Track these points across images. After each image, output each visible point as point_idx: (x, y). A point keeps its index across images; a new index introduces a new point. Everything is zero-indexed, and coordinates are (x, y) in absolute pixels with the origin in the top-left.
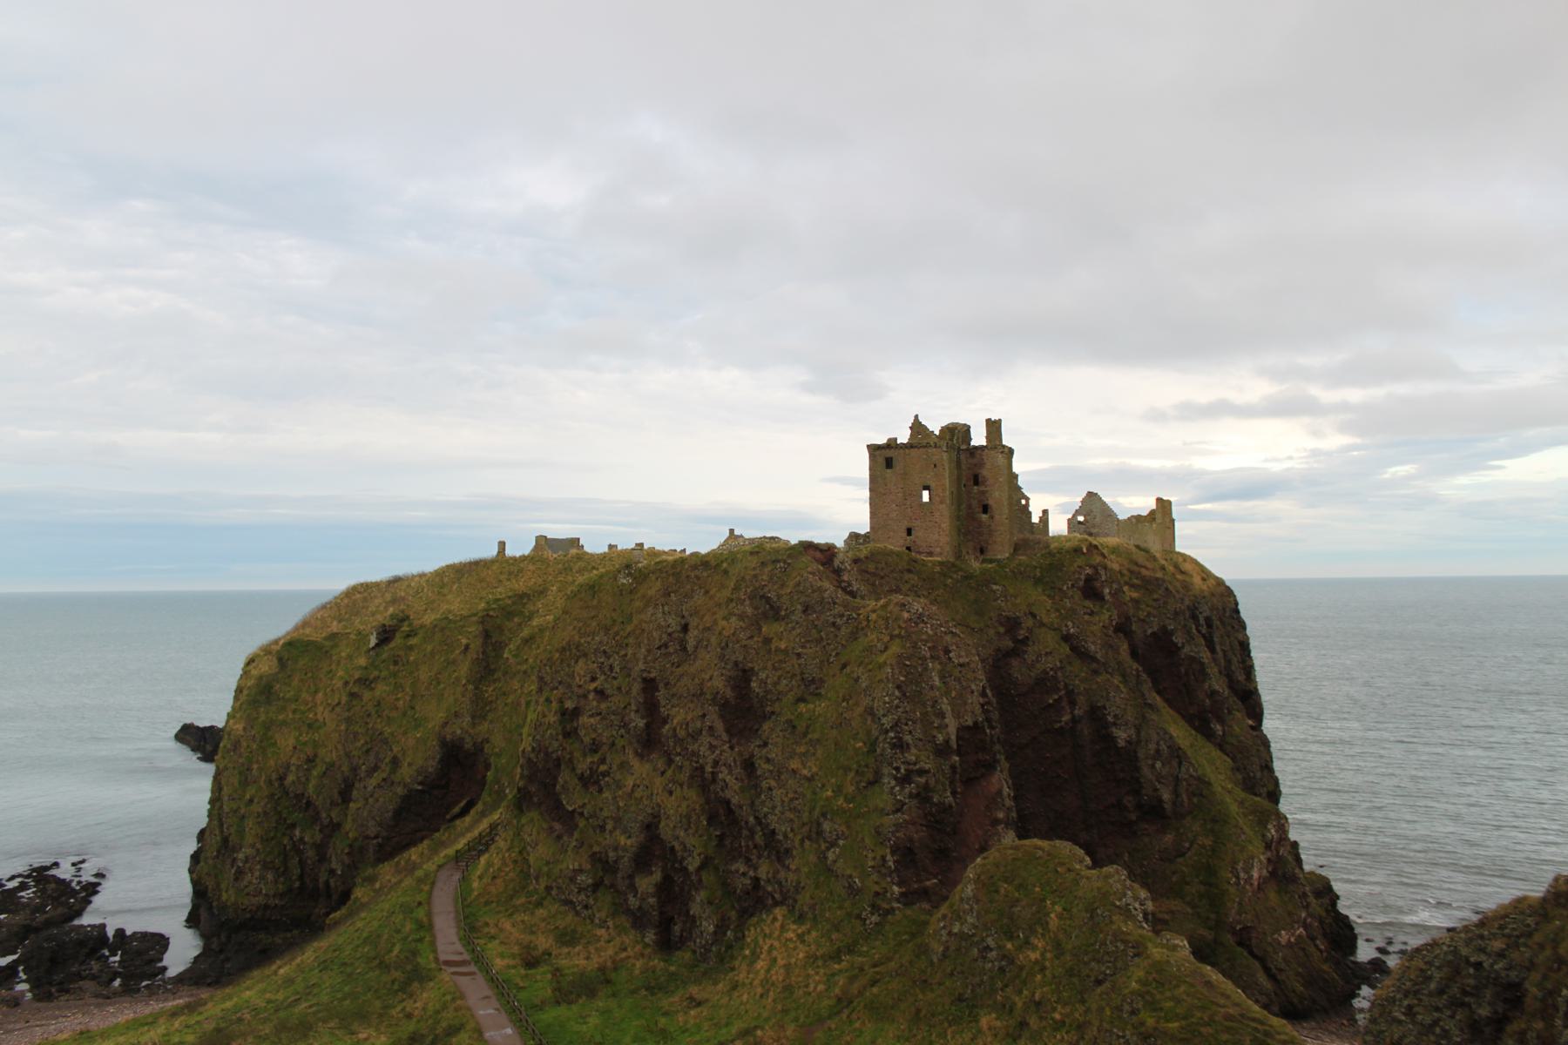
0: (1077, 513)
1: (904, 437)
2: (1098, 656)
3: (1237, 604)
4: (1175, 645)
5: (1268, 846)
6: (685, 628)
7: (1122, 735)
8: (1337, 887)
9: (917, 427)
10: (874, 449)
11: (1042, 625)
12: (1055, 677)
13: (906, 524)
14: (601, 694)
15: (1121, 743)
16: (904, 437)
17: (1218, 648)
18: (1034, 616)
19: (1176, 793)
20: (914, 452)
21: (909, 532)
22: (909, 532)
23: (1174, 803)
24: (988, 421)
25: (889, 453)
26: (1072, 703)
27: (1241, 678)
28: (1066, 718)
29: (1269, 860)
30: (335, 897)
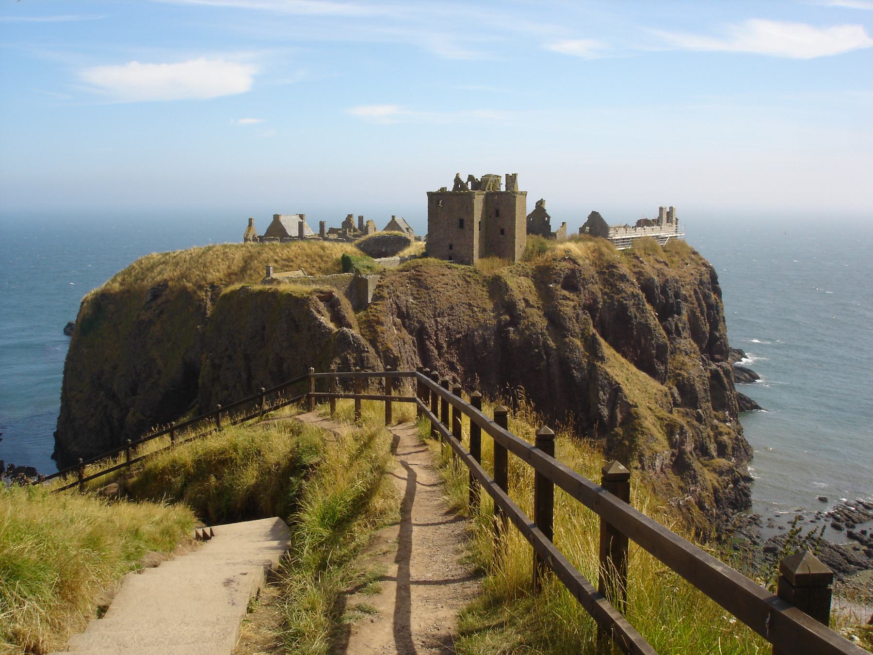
0: (585, 225)
1: (450, 188)
3: (714, 278)
4: (630, 318)
5: (672, 445)
6: (264, 328)
9: (457, 180)
10: (430, 195)
11: (532, 307)
12: (538, 338)
14: (230, 357)
16: (450, 188)
17: (684, 312)
18: (526, 301)
21: (451, 247)
22: (451, 247)
24: (507, 175)
26: (548, 354)
27: (707, 328)
28: (543, 363)
29: (673, 455)
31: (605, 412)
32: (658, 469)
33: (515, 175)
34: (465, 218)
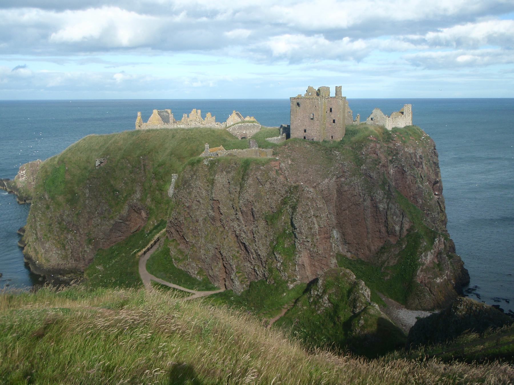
2: (374, 177)
7: (381, 206)
8: (463, 259)
13: (304, 128)
15: (381, 209)
19: (401, 228)
20: (308, 101)
21: (305, 131)
22: (305, 131)
23: (400, 231)
25: (299, 101)
30: (87, 261)
31: (397, 228)
32: (428, 261)
33: (341, 87)
34: (315, 114)
